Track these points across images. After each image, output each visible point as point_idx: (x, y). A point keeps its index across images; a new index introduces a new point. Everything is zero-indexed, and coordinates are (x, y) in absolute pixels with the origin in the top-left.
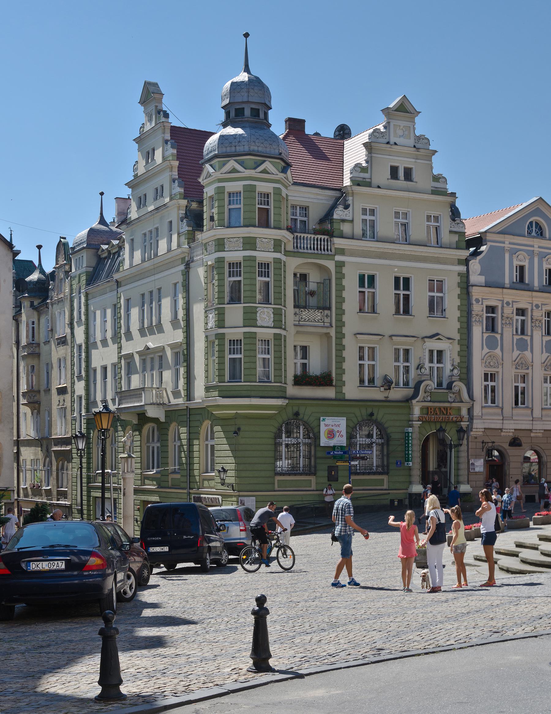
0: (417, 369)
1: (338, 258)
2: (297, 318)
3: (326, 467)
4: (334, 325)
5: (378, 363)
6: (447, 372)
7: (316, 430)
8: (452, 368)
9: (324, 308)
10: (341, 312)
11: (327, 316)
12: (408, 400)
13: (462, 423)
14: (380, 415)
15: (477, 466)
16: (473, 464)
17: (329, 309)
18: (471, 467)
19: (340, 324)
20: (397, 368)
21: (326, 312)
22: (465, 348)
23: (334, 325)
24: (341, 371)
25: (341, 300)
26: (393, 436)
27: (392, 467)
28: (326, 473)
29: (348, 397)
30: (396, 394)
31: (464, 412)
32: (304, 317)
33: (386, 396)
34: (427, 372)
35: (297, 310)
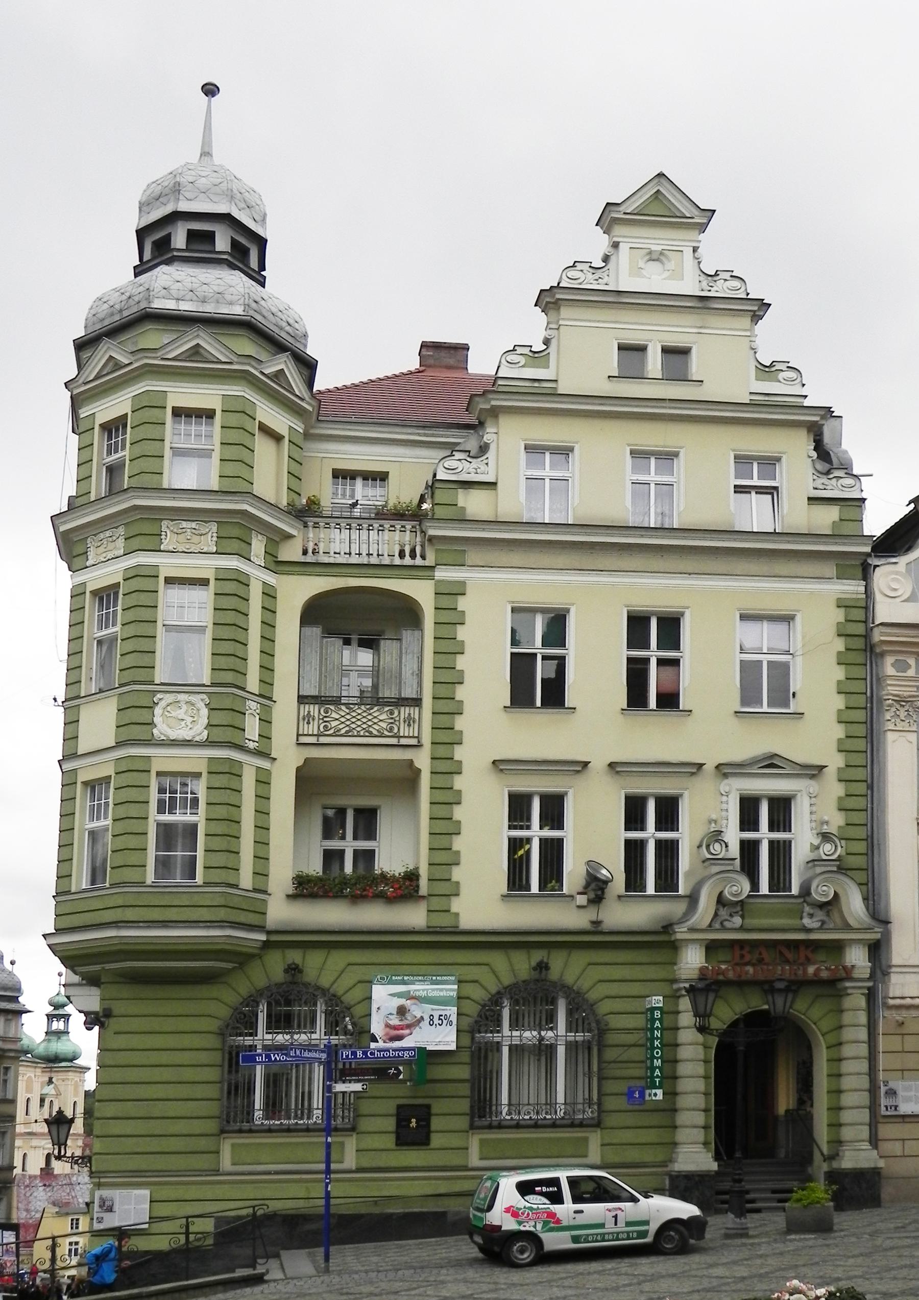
0: (700, 846)
1: (441, 574)
2: (313, 728)
3: (390, 1107)
4: (426, 739)
5: (570, 834)
6: (800, 854)
7: (358, 1011)
8: (816, 842)
9: (402, 702)
10: (449, 709)
11: (409, 721)
12: (667, 928)
13: (848, 984)
14: (567, 968)
15: (907, 1100)
16: (892, 1093)
17: (417, 702)
18: (884, 1101)
19: (447, 737)
20: (634, 851)
21: (405, 711)
22: (861, 788)
23: (426, 739)
24: (444, 856)
25: (449, 679)
26: (616, 1022)
27: (611, 1103)
28: (390, 1124)
29: (466, 923)
30: (627, 914)
31: (857, 958)
32: (334, 724)
33: (594, 918)
34: (735, 851)
35: (314, 709)
